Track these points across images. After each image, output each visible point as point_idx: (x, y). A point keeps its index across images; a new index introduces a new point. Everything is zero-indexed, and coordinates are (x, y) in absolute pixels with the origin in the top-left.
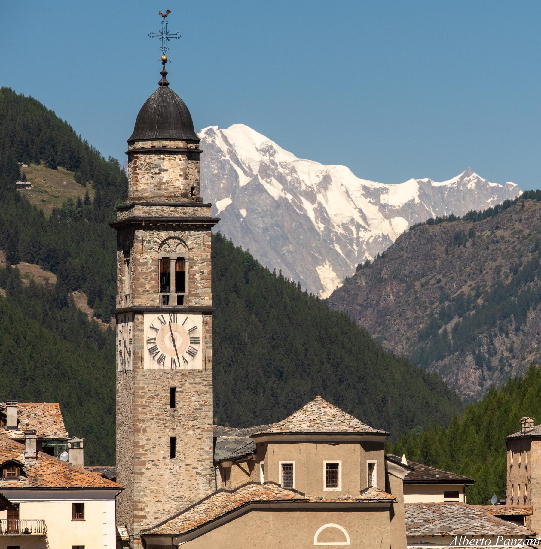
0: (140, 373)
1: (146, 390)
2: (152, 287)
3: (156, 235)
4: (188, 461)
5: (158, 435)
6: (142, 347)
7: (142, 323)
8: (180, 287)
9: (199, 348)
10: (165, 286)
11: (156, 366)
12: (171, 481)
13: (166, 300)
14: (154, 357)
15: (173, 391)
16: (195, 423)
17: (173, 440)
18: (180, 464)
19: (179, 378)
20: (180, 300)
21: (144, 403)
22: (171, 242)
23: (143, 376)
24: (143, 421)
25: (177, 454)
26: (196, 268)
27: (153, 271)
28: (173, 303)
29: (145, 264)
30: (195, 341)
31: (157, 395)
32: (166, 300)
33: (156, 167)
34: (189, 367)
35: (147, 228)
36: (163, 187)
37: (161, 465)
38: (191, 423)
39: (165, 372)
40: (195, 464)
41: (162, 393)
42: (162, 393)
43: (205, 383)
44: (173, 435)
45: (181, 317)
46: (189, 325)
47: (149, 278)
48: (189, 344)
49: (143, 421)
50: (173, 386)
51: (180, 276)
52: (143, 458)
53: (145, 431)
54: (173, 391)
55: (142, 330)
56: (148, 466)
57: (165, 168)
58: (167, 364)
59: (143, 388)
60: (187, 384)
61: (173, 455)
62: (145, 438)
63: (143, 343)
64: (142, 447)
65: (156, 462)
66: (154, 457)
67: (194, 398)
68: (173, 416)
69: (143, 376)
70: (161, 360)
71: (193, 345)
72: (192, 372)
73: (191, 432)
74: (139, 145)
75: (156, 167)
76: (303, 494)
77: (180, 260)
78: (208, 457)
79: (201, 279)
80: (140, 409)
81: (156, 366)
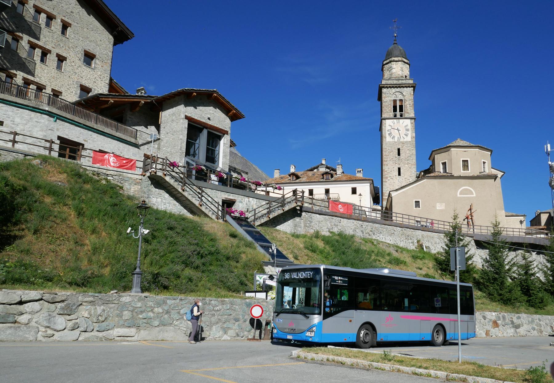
0: (385, 143)
1: (387, 149)
2: (389, 110)
3: (390, 91)
4: (406, 177)
5: (393, 167)
6: (385, 133)
7: (385, 124)
8: (401, 110)
9: (409, 133)
10: (395, 110)
11: (391, 140)
12: (398, 185)
13: (395, 116)
14: (390, 137)
15: (399, 150)
16: (408, 162)
17: (399, 169)
18: (403, 178)
19: (401, 144)
20: (401, 115)
21: (387, 154)
22: (396, 93)
23: (386, 144)
24: (386, 161)
25: (401, 174)
26: (407, 103)
27: (389, 104)
28: (398, 116)
29: (387, 102)
30: (407, 130)
31: (392, 151)
32: (395, 116)
33: (391, 67)
34: (405, 140)
35: (387, 87)
36: (393, 74)
37: (394, 178)
38: (406, 162)
39: (395, 142)
40: (409, 178)
41: (394, 150)
42: (394, 150)
43: (412, 146)
44: (399, 167)
45: (401, 121)
46: (405, 124)
47: (388, 107)
48: (405, 131)
49: (386, 161)
50: (399, 147)
51: (401, 107)
52: (387, 176)
53: (387, 165)
54: (399, 150)
55: (385, 126)
56: (388, 179)
57: (394, 67)
58: (396, 139)
59: (386, 148)
60: (404, 147)
61: (399, 174)
62: (387, 168)
63: (386, 131)
64: (386, 171)
65: (392, 177)
66: (391, 175)
67: (407, 152)
68: (399, 159)
69: (386, 144)
70: (393, 138)
71: (407, 132)
72: (406, 142)
73: (407, 165)
74: (385, 63)
75: (391, 67)
76: (452, 174)
77: (401, 100)
78: (414, 175)
79: (410, 107)
80: (385, 157)
81: (391, 140)
